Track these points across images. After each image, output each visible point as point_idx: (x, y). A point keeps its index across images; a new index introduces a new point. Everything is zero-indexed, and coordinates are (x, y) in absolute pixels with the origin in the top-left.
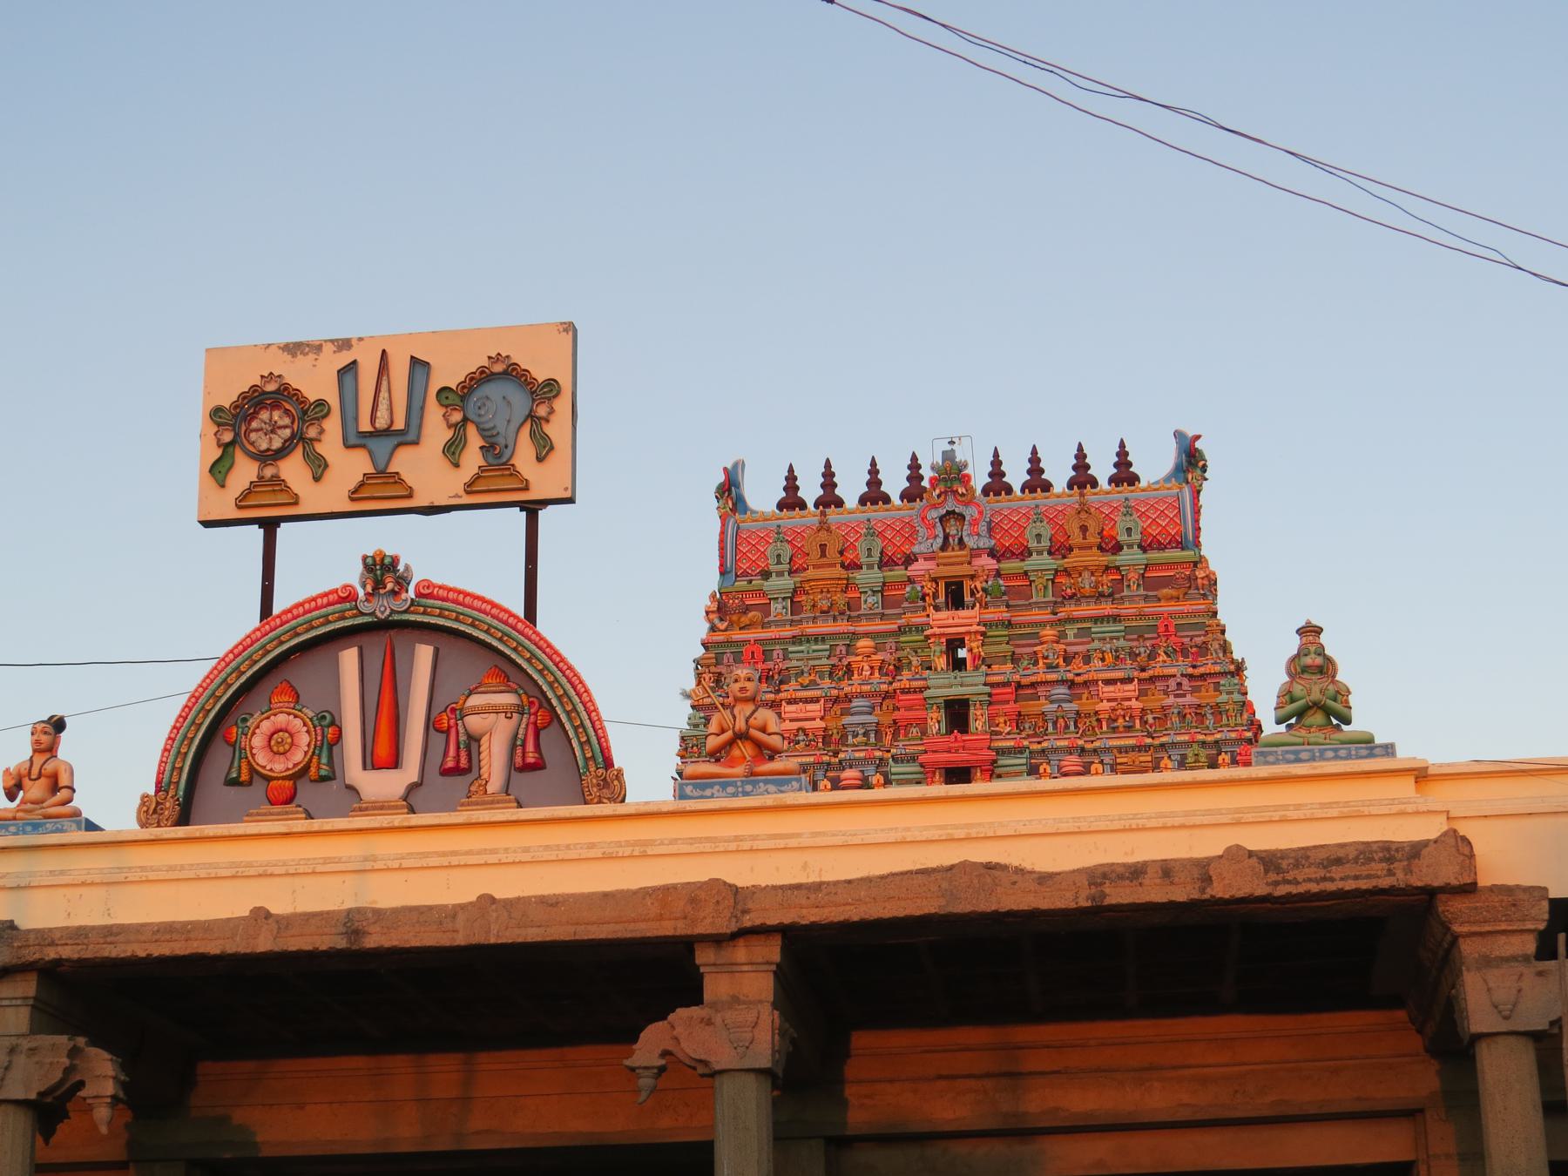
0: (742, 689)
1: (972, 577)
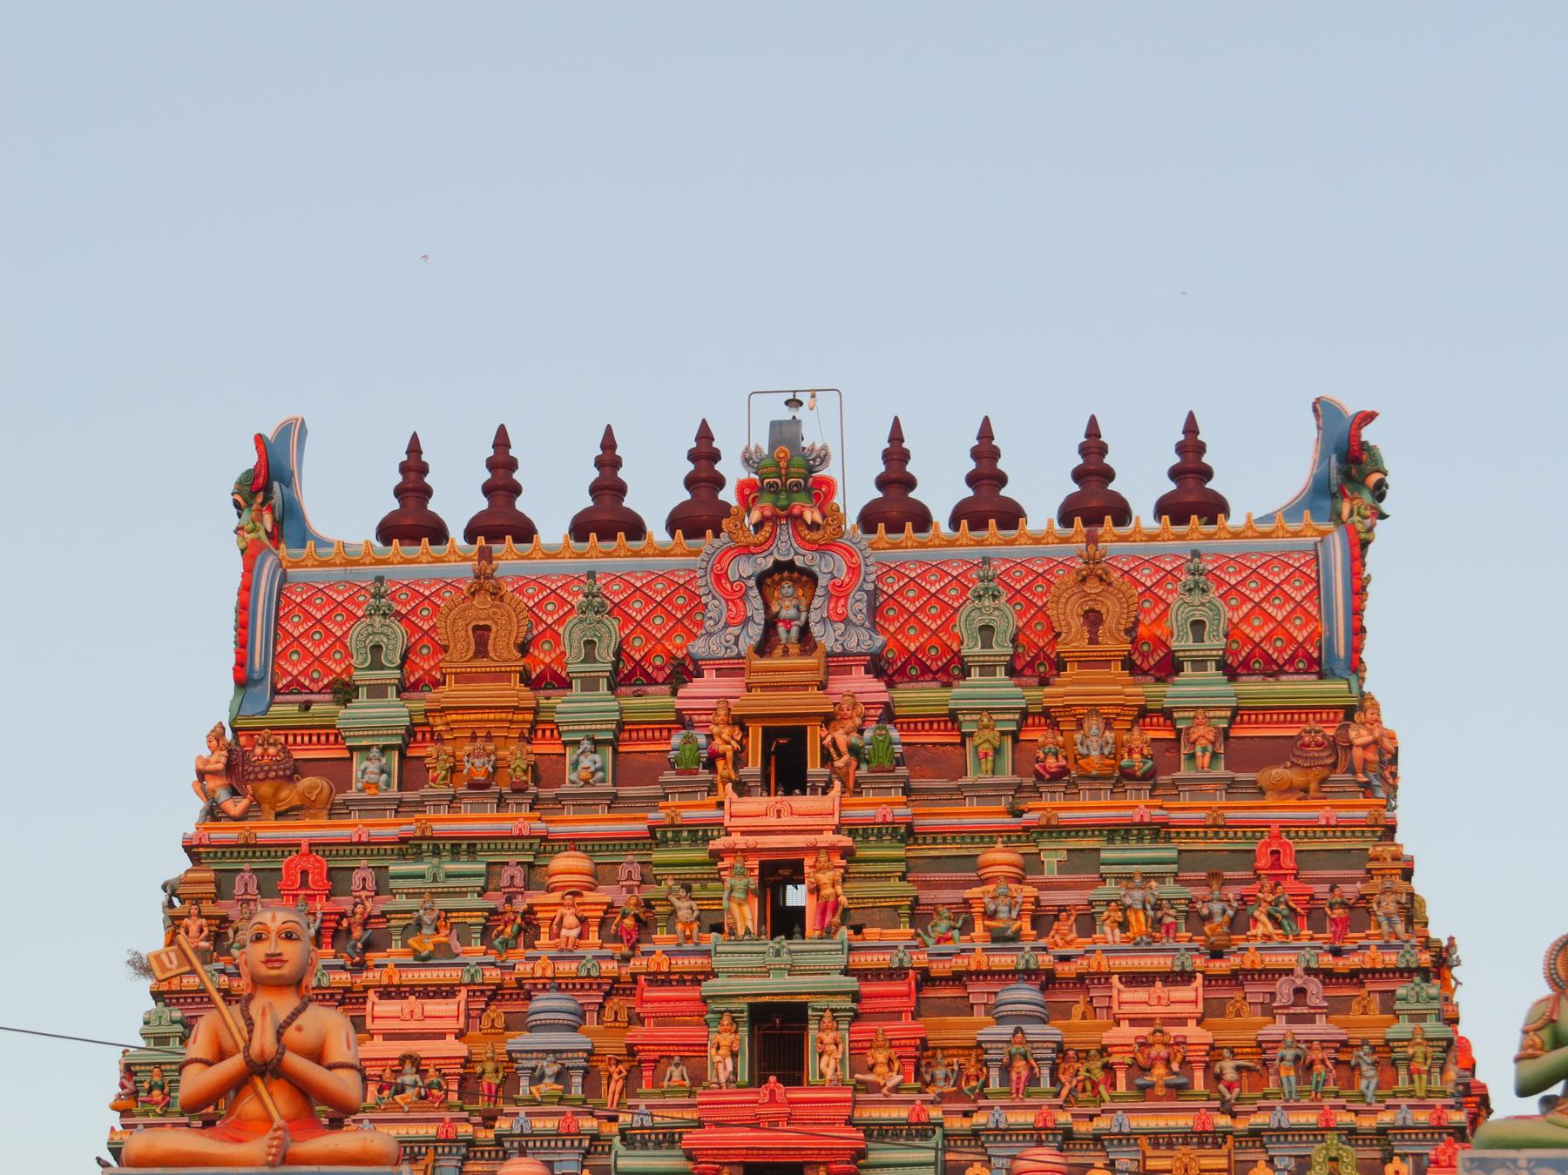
0: (272, 959)
1: (828, 720)
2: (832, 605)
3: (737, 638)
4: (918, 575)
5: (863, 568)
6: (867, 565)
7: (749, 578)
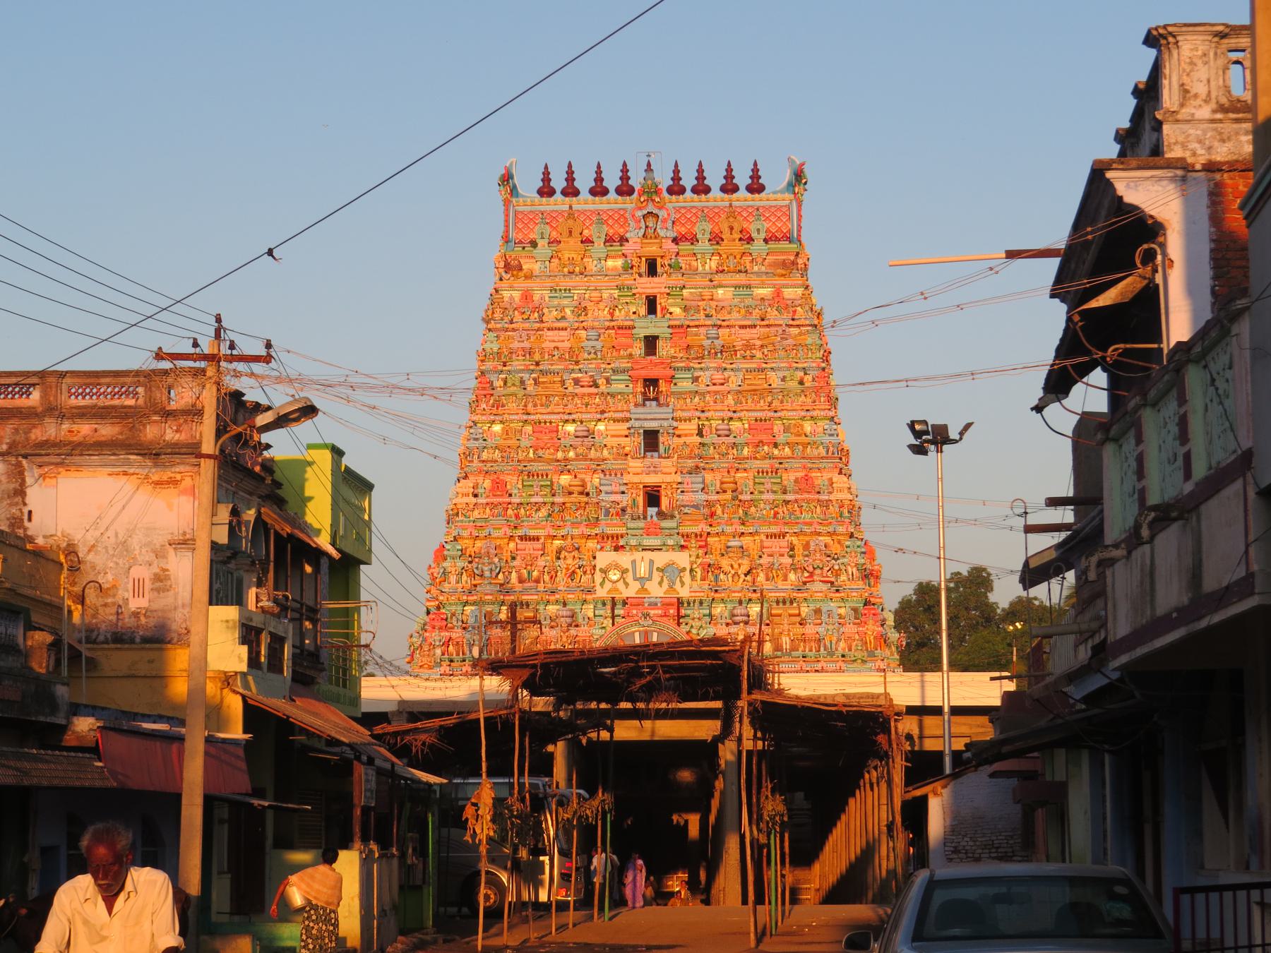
1: (662, 257)
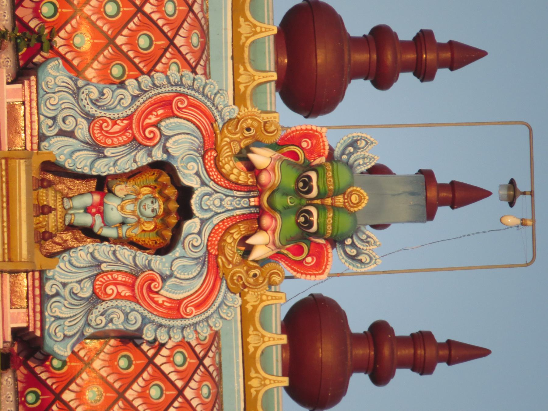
2: (120, 278)
3: (71, 134)
4: (188, 402)
5: (179, 323)
6: (183, 328)
7: (166, 151)
